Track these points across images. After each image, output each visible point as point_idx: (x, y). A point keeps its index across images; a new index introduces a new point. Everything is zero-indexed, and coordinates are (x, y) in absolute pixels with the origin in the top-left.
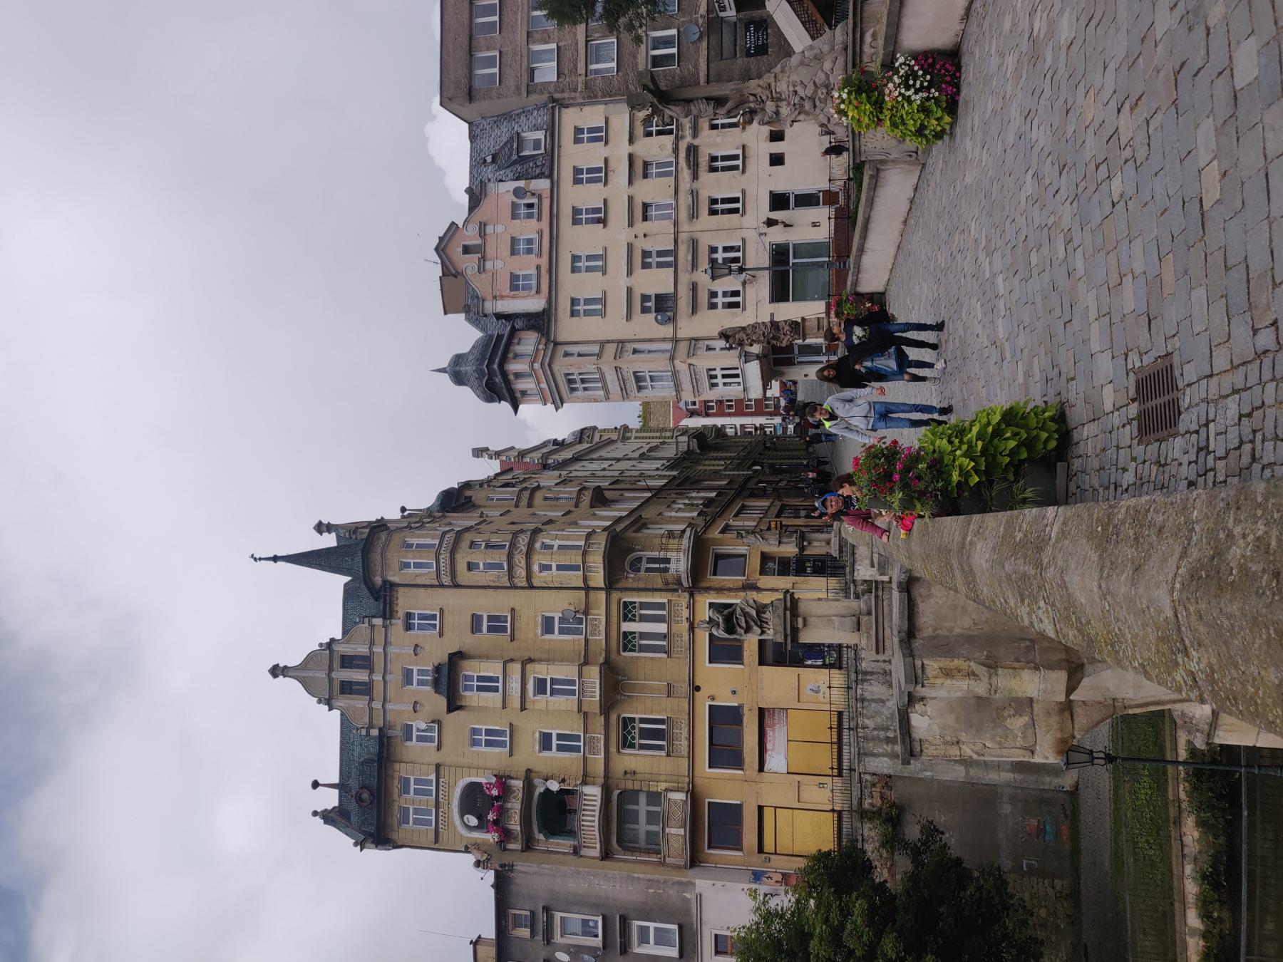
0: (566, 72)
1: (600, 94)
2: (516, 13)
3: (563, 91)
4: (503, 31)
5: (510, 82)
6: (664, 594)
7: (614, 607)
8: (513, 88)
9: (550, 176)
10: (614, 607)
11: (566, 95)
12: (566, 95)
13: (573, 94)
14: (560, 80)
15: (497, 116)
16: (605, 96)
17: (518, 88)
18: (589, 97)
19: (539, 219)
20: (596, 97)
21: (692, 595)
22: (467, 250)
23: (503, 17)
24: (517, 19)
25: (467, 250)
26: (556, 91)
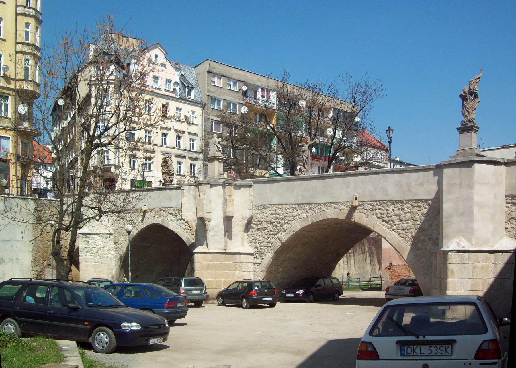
0: (213, 112)
1: (205, 124)
2: (233, 97)
3: (207, 109)
4: (228, 90)
5: (212, 89)
6: (14, 117)
7: (8, 92)
8: (210, 90)
9: (180, 98)
10: (8, 92)
11: (206, 110)
12: (206, 110)
13: (206, 113)
14: (211, 109)
15: (197, 80)
16: (204, 125)
17: (210, 92)
18: (205, 119)
19: (166, 90)
20: (204, 122)
21: (14, 130)
22: (156, 56)
23: (232, 91)
24: (231, 97)
25: (156, 56)
26: (207, 107)
